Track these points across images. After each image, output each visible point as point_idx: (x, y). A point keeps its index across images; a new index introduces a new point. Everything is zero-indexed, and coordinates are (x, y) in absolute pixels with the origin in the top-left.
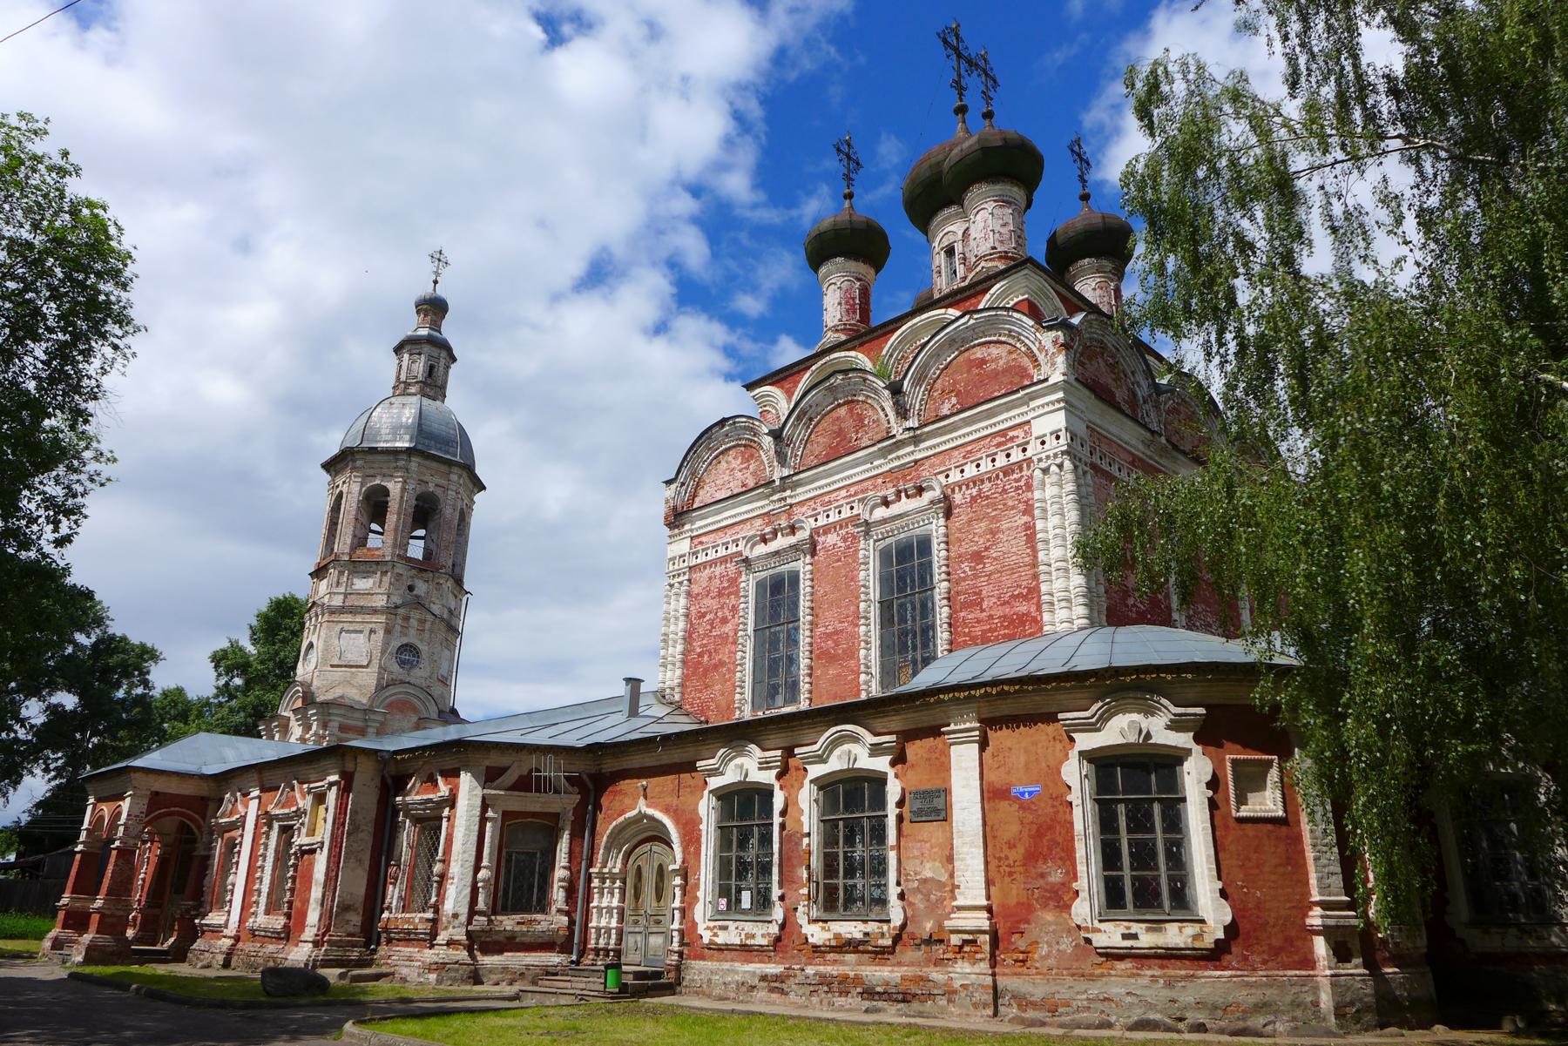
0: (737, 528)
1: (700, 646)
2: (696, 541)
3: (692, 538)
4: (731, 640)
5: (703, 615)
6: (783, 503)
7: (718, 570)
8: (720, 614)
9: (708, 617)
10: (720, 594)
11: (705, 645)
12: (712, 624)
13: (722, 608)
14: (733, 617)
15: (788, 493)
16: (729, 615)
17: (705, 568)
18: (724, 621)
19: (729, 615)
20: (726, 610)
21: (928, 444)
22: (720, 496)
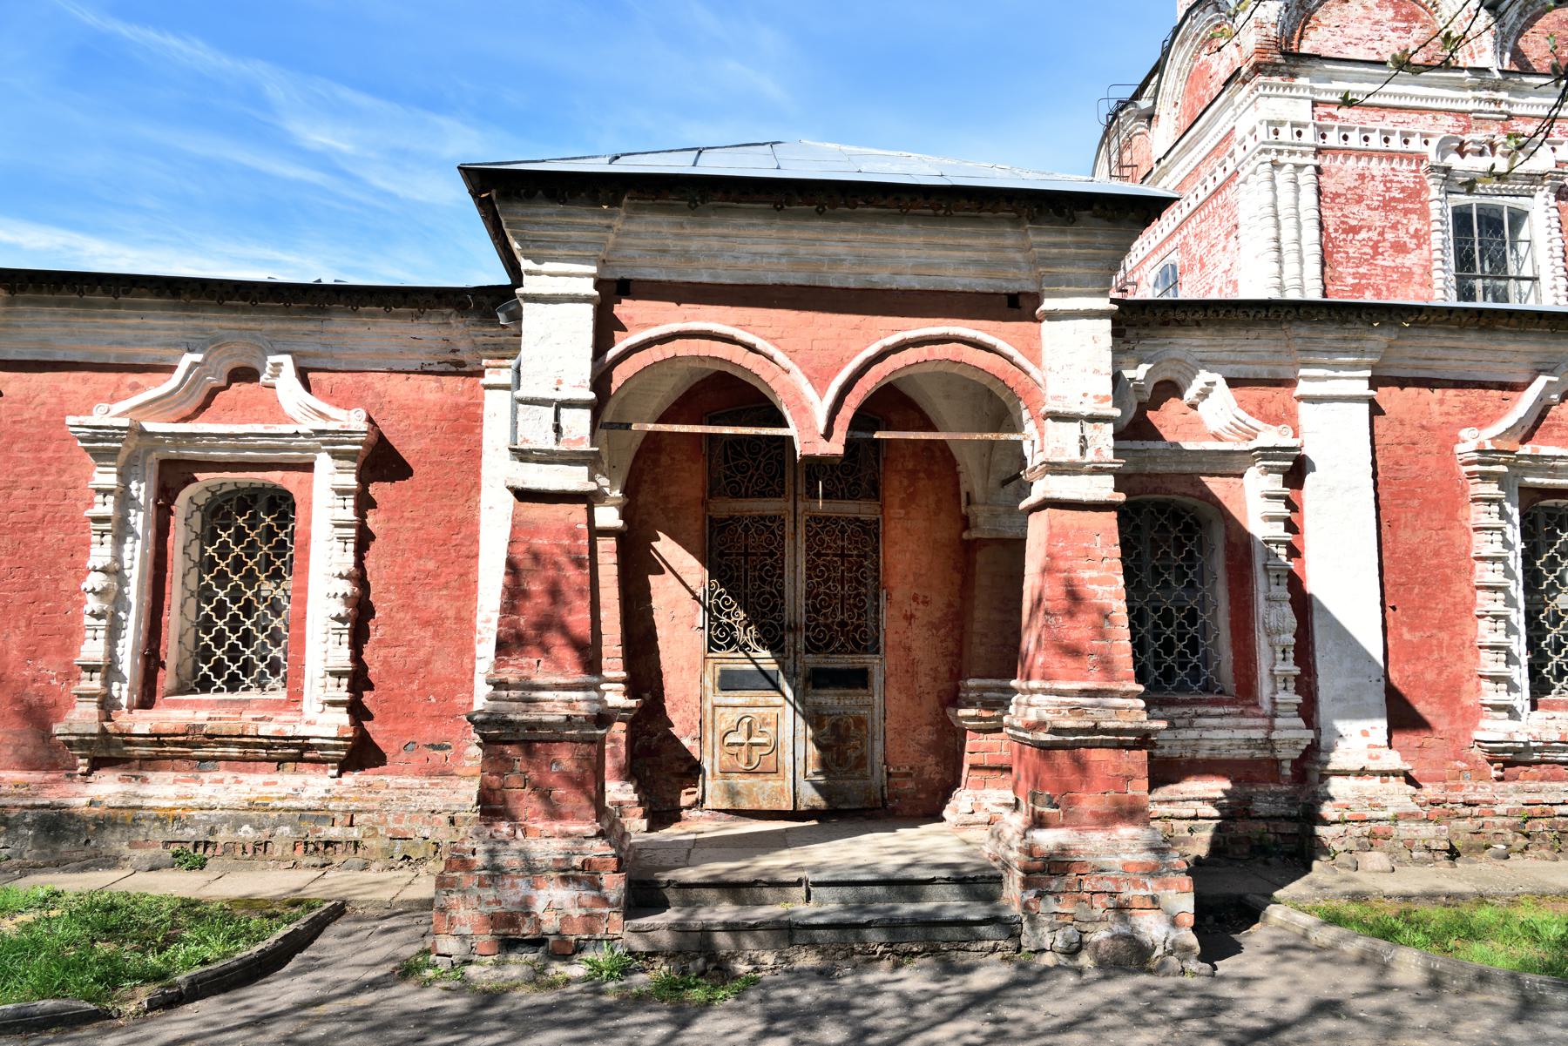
0: (1404, 116)
1: (1354, 275)
2: (1320, 110)
3: (1315, 104)
4: (1417, 279)
5: (1355, 230)
6: (1492, 107)
7: (1377, 168)
8: (1390, 236)
9: (1363, 235)
10: (1387, 205)
11: (1363, 276)
12: (1375, 247)
13: (1394, 227)
14: (1419, 246)
15: (1503, 95)
16: (1412, 243)
17: (1358, 158)
18: (1400, 248)
19: (1412, 243)
20: (1402, 233)
21: (1531, 100)
22: (1351, 53)
